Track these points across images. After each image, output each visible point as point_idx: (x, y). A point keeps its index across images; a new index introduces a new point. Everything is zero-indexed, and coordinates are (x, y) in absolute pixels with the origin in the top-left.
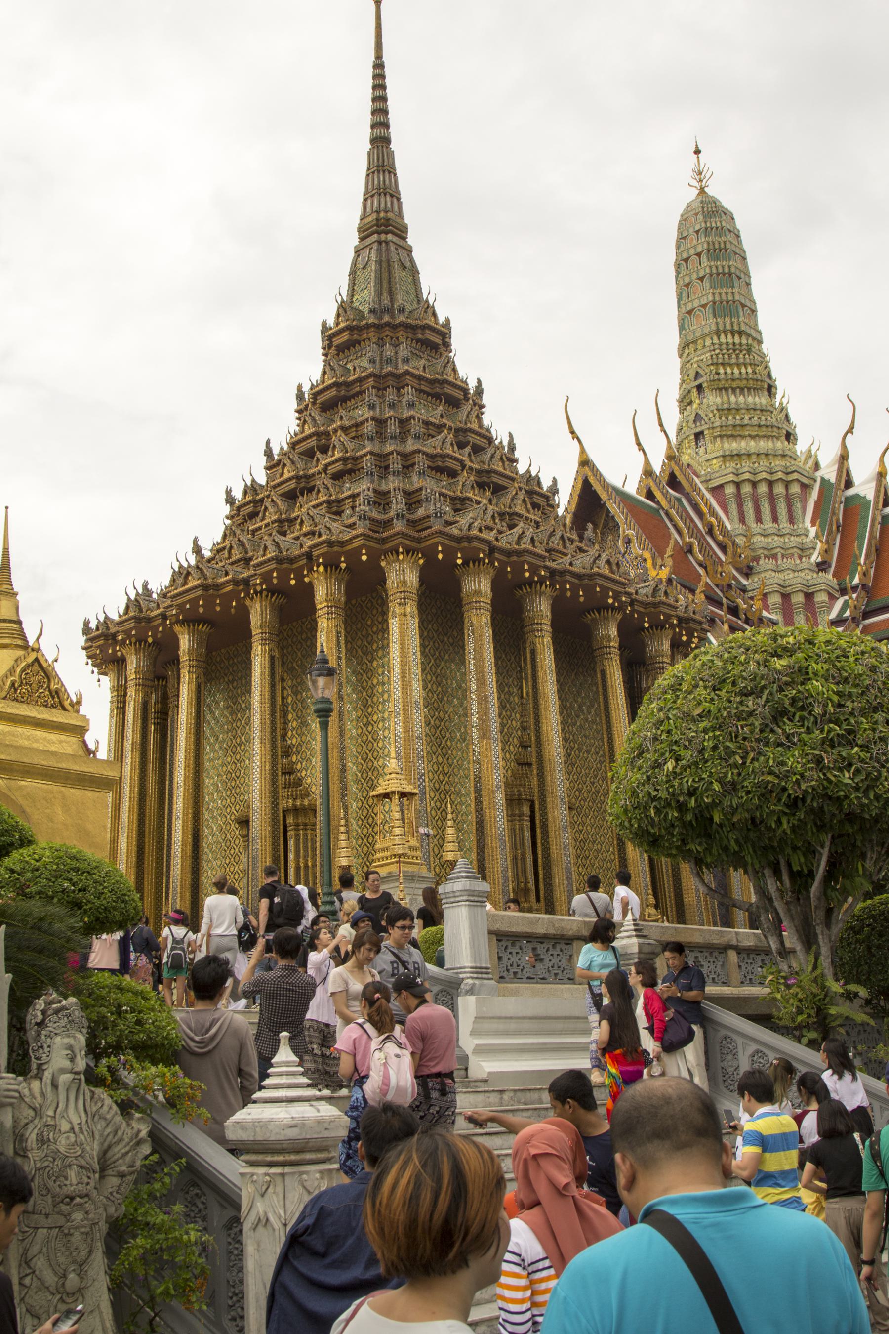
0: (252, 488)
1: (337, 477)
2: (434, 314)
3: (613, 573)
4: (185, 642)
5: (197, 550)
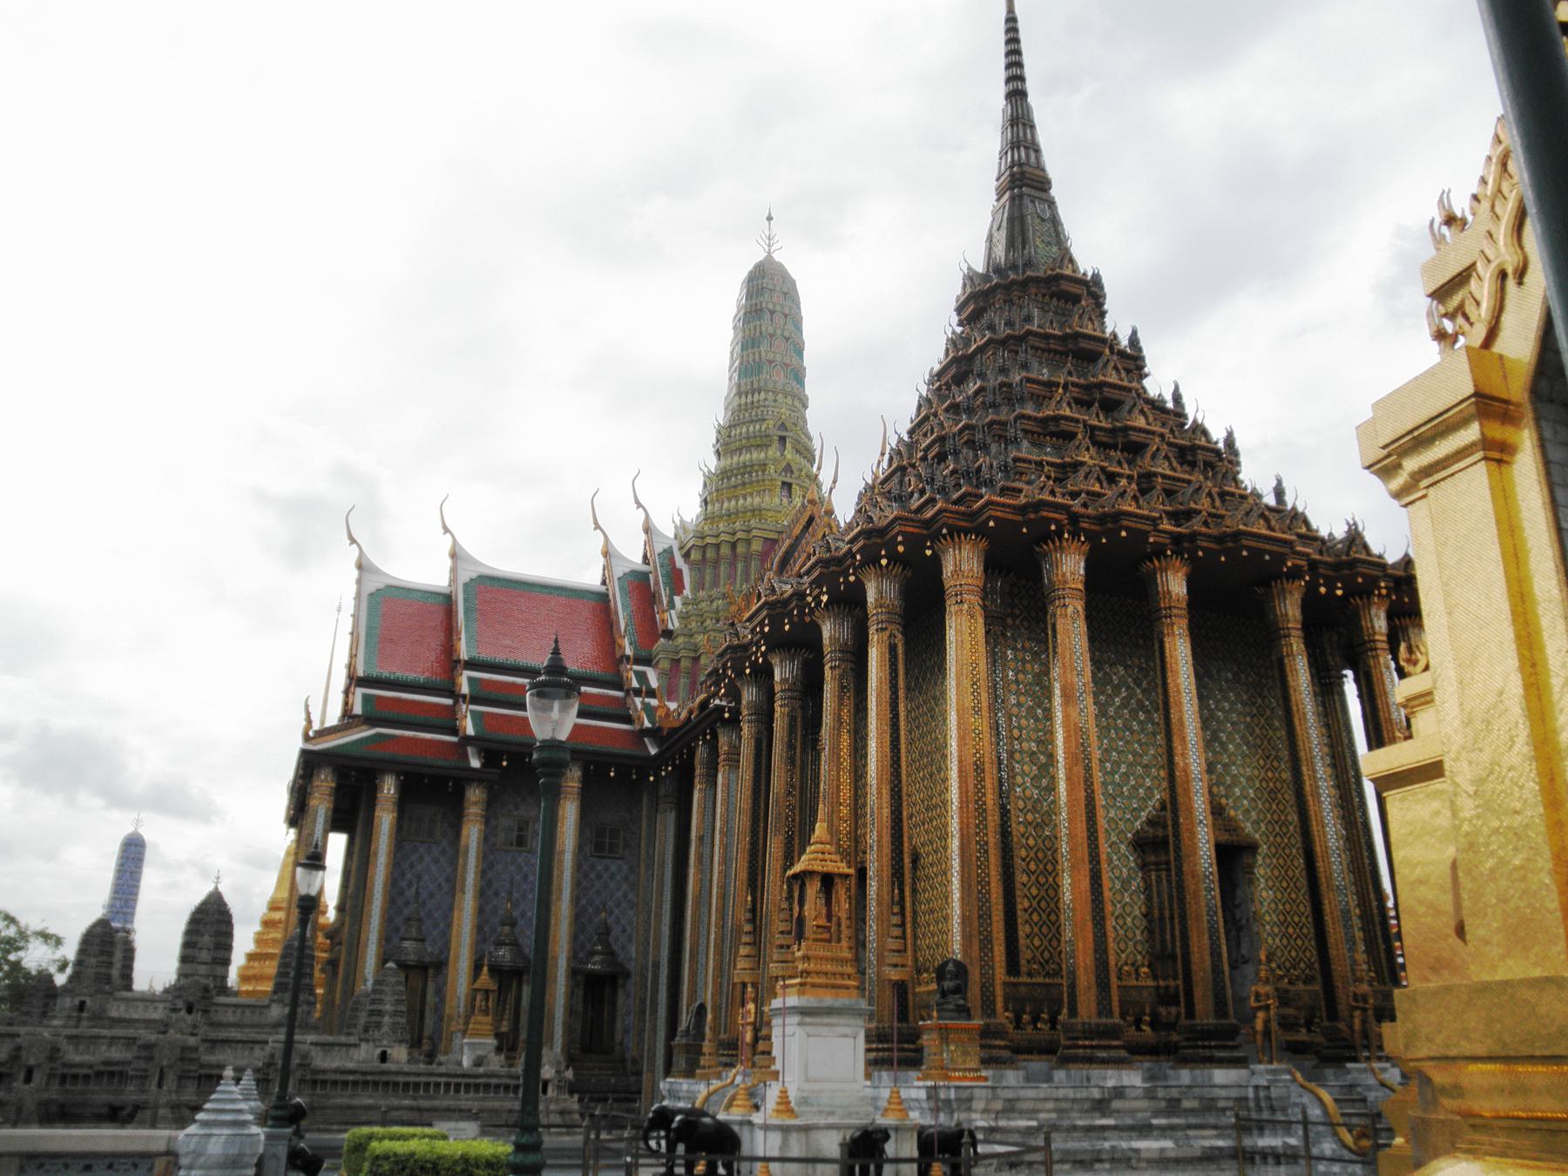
2: (1071, 260)
3: (1273, 530)
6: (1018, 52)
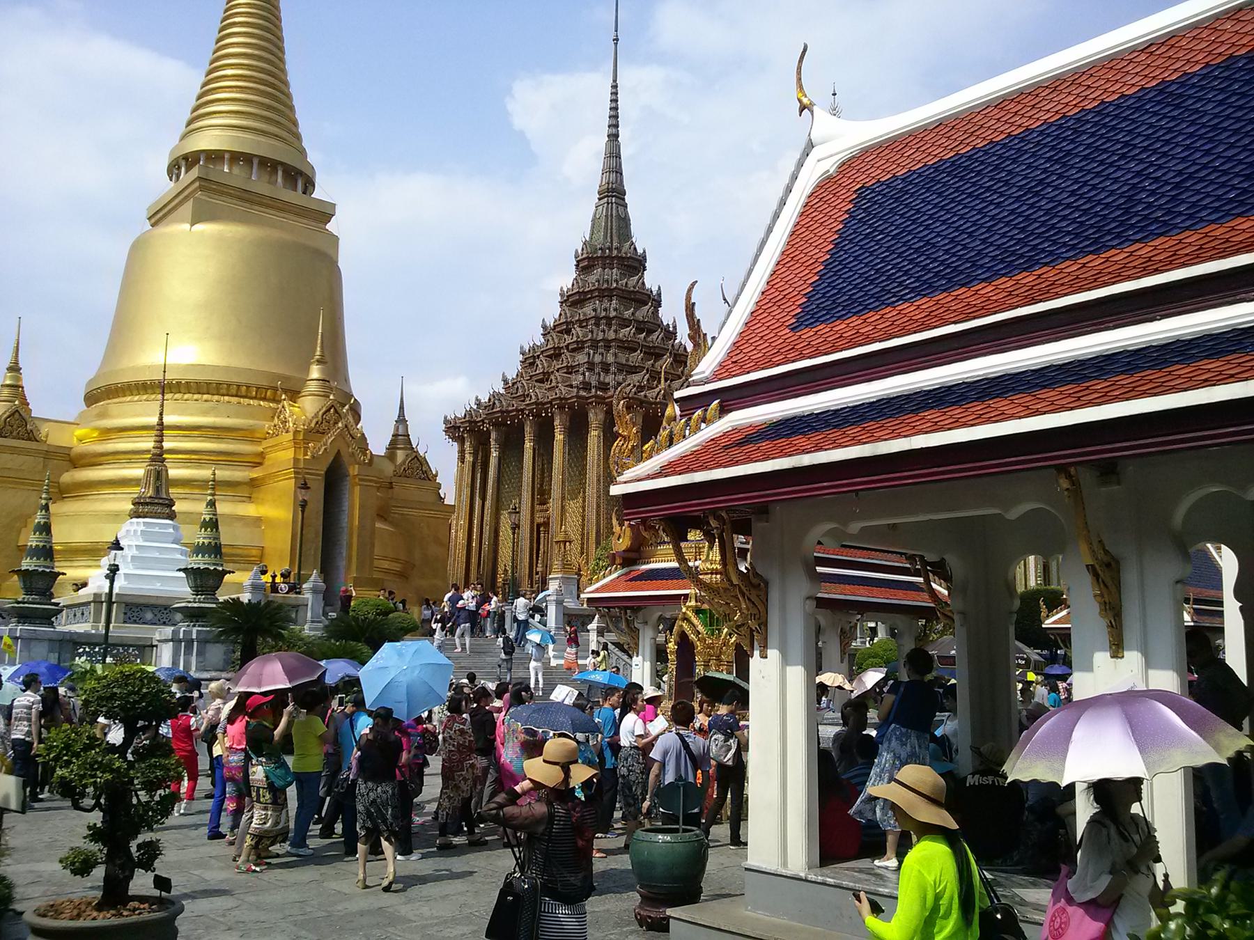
0: (533, 348)
1: (574, 350)
4: (493, 435)
5: (505, 381)
6: (616, 109)
